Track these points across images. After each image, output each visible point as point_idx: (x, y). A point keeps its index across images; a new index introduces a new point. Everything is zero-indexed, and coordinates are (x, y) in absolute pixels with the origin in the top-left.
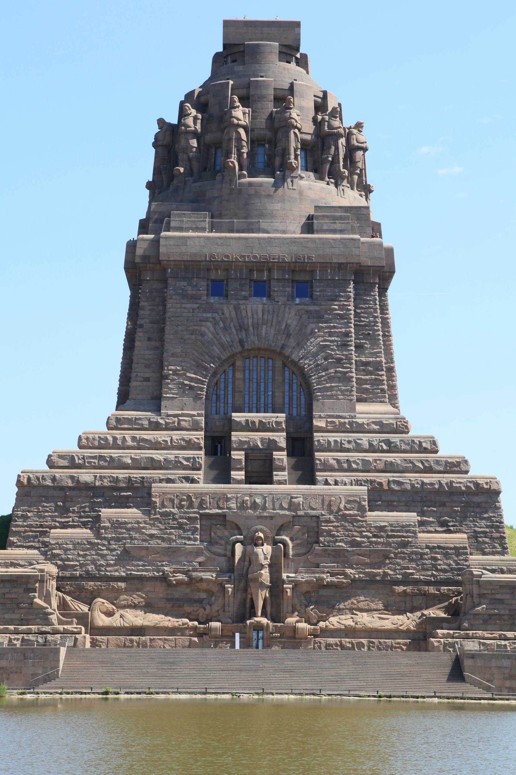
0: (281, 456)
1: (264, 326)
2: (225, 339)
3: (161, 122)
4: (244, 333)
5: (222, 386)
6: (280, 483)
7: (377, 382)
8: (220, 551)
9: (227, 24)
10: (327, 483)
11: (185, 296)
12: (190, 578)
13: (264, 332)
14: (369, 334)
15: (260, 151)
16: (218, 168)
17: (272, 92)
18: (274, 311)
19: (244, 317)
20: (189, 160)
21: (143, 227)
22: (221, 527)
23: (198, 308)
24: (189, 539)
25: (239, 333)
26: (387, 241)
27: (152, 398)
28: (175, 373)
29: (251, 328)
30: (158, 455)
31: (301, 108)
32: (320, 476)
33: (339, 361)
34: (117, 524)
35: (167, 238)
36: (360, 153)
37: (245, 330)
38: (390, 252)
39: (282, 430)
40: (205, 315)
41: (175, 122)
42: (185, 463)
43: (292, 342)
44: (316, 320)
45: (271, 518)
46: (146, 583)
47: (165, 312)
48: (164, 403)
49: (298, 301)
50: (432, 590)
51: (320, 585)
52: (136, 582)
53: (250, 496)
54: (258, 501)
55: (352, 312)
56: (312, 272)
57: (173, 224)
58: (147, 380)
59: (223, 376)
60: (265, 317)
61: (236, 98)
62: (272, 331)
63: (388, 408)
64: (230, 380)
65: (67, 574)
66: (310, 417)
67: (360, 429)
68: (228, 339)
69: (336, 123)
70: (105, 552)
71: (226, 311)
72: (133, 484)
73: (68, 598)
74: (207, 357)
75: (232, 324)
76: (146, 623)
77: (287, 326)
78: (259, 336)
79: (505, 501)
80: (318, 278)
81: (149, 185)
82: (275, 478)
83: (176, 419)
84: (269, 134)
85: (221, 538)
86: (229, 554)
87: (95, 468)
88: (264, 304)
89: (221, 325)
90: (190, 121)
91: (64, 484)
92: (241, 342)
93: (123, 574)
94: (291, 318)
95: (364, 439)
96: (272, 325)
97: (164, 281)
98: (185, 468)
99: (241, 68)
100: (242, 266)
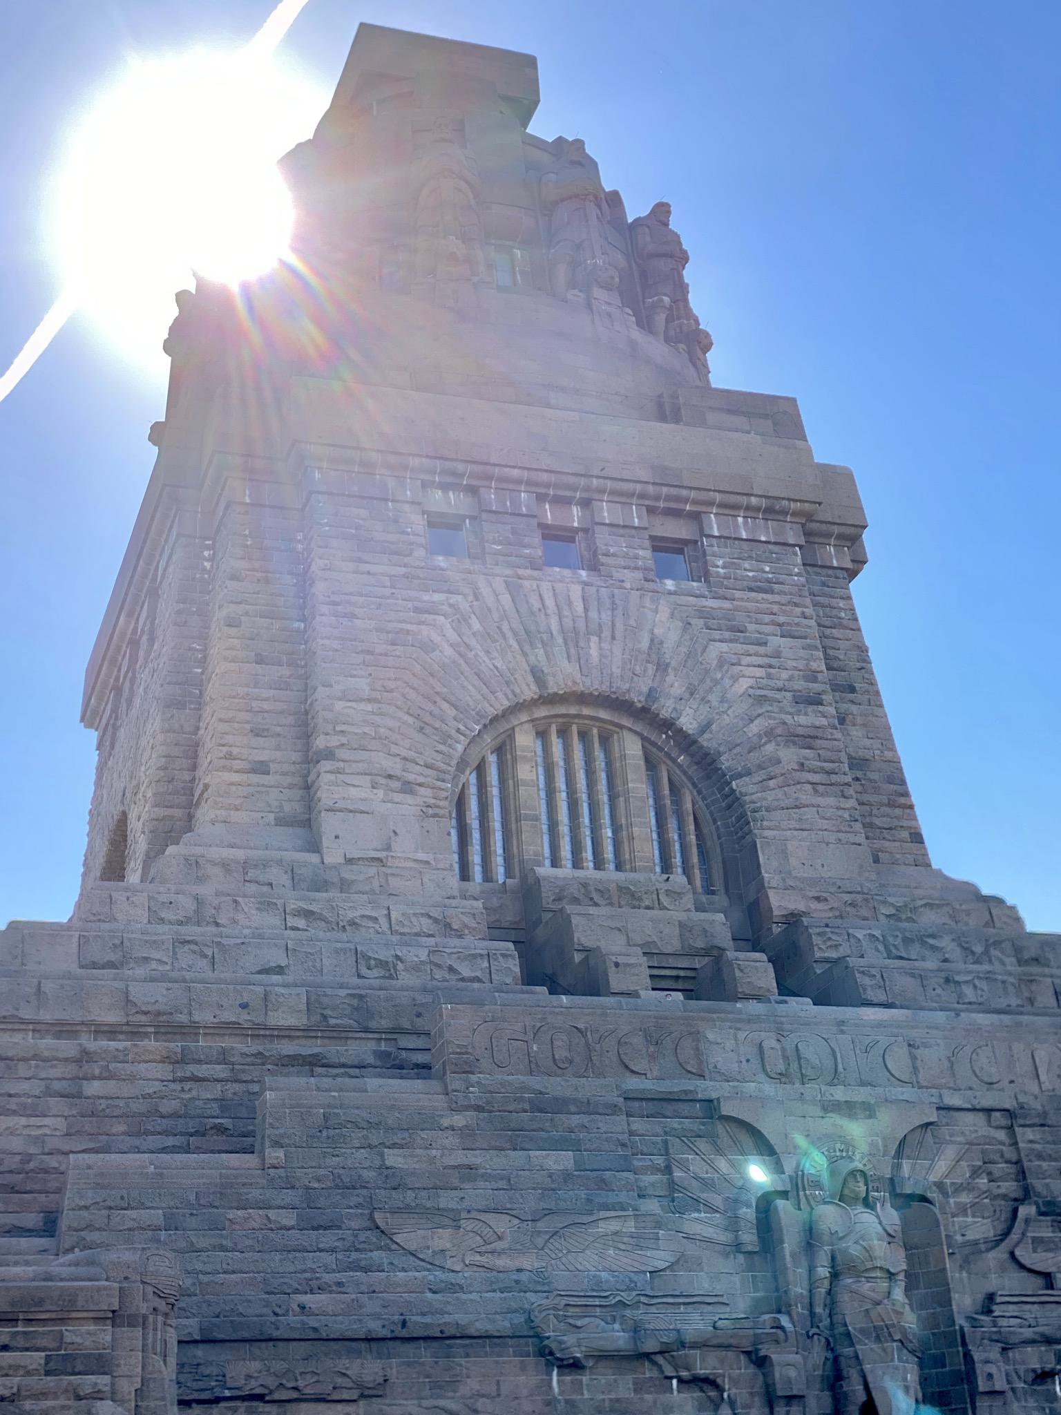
1: (594, 639)
4: (541, 652)
7: (898, 811)
8: (709, 1232)
13: (594, 652)
14: (852, 690)
18: (613, 603)
19: (535, 609)
22: (702, 1145)
23: (406, 576)
24: (603, 1185)
25: (527, 648)
27: (281, 822)
29: (560, 641)
33: (806, 739)
37: (544, 644)
40: (426, 597)
44: (727, 635)
46: (462, 1361)
48: (329, 824)
49: (670, 584)
52: (425, 1354)
54: (806, 1052)
55: (813, 623)
56: (696, 517)
58: (261, 768)
59: (473, 779)
60: (593, 614)
62: (617, 651)
64: (495, 791)
68: (499, 664)
70: (295, 1237)
71: (485, 591)
72: (325, 1017)
74: (445, 706)
75: (505, 627)
77: (656, 644)
78: (581, 660)
80: (716, 534)
83: (372, 871)
85: (707, 1184)
86: (749, 1238)
88: (586, 584)
89: (476, 626)
92: (538, 677)
93: (375, 1327)
96: (613, 638)
100: (519, 482)
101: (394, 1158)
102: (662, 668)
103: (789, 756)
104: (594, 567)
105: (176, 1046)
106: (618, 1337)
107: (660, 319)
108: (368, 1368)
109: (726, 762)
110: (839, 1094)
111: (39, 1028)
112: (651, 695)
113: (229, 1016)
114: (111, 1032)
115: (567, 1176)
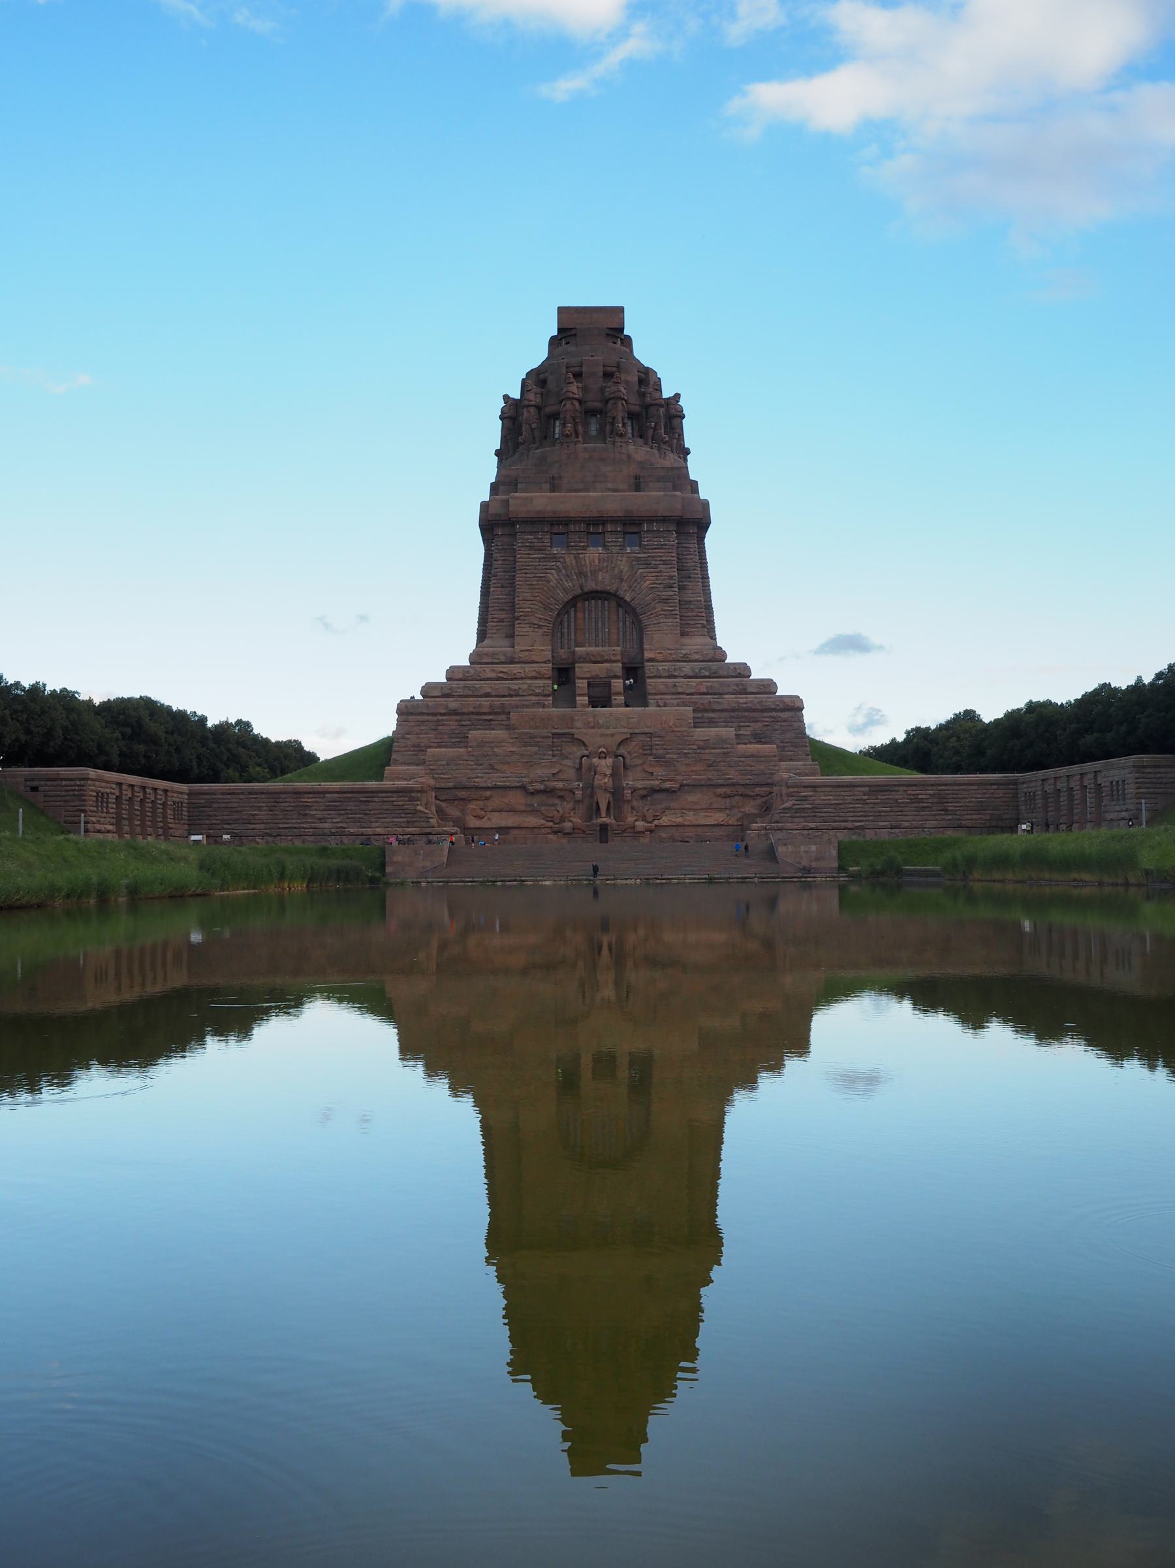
0: (618, 685)
2: (568, 584)
3: (506, 397)
5: (566, 624)
6: (619, 706)
9: (561, 310)
10: (659, 706)
11: (531, 548)
12: (546, 786)
15: (593, 421)
16: (557, 436)
17: (601, 369)
20: (532, 430)
21: (494, 488)
26: (703, 495)
27: (506, 637)
28: (526, 614)
30: (514, 685)
31: (627, 382)
32: (652, 700)
33: (665, 601)
34: (482, 744)
35: (514, 498)
36: (676, 420)
38: (705, 505)
39: (617, 661)
41: (518, 397)
42: (537, 691)
43: (625, 586)
45: (612, 735)
47: (515, 562)
48: (517, 639)
50: (747, 791)
51: (653, 791)
52: (501, 791)
53: (594, 716)
56: (640, 524)
57: (519, 486)
58: (502, 620)
61: (571, 375)
63: (708, 640)
65: (443, 785)
66: (642, 650)
67: (686, 659)
69: (657, 395)
71: (567, 560)
73: (444, 805)
76: (510, 825)
79: (808, 716)
81: (497, 453)
82: (614, 702)
84: (598, 405)
86: (577, 766)
87: (461, 696)
90: (531, 396)
91: (436, 711)
92: (581, 587)
94: (623, 565)
95: (687, 668)
97: (513, 535)
98: (537, 695)
99: (574, 348)
101: (496, 750)
102: (622, 580)
103: (659, 607)
104: (605, 546)
105: (458, 717)
106: (542, 787)
107: (651, 432)
108: (488, 793)
109: (638, 610)
110: (608, 732)
111: (428, 714)
112: (617, 591)
113: (471, 710)
114: (444, 714)
115: (536, 753)
